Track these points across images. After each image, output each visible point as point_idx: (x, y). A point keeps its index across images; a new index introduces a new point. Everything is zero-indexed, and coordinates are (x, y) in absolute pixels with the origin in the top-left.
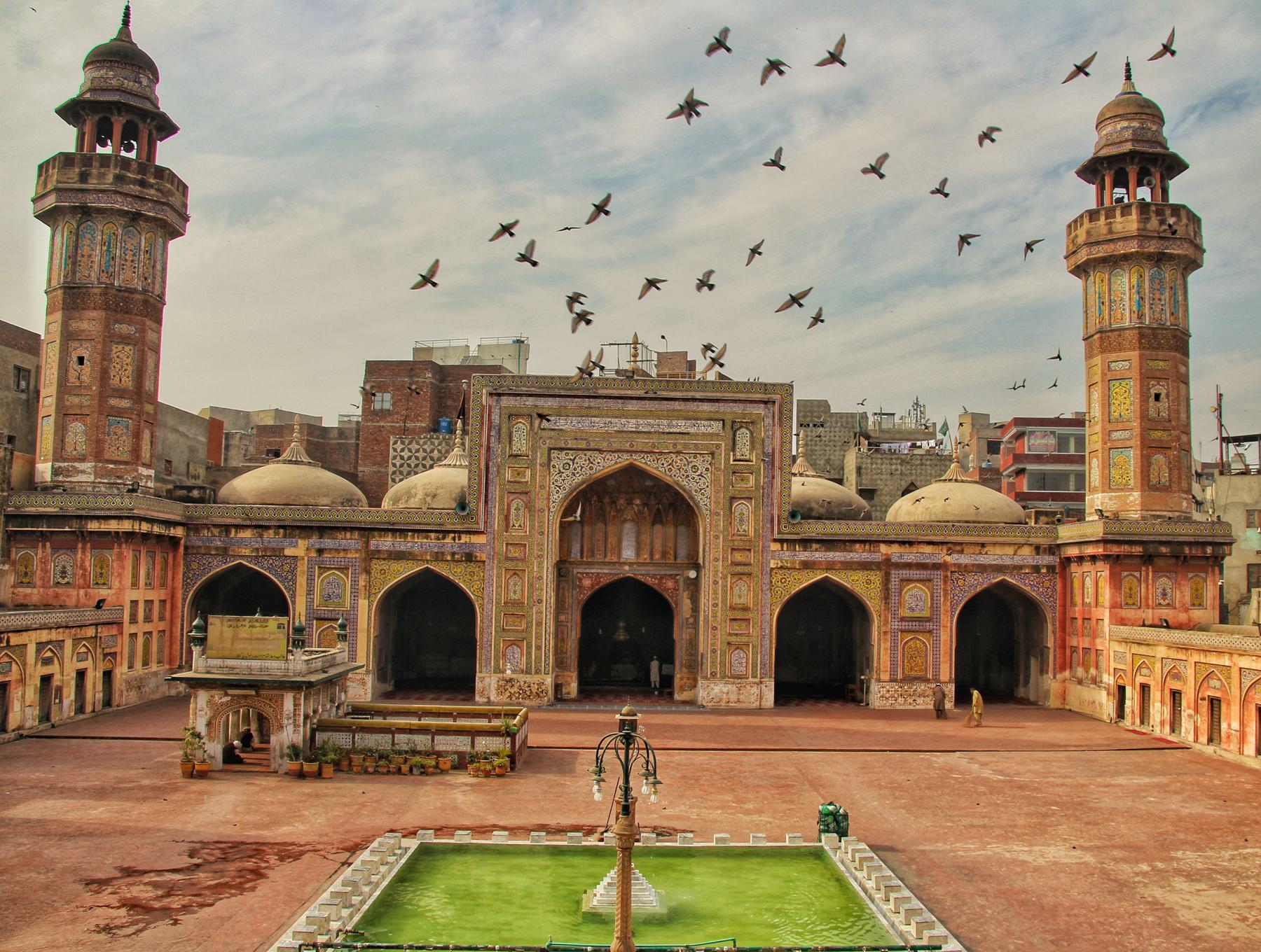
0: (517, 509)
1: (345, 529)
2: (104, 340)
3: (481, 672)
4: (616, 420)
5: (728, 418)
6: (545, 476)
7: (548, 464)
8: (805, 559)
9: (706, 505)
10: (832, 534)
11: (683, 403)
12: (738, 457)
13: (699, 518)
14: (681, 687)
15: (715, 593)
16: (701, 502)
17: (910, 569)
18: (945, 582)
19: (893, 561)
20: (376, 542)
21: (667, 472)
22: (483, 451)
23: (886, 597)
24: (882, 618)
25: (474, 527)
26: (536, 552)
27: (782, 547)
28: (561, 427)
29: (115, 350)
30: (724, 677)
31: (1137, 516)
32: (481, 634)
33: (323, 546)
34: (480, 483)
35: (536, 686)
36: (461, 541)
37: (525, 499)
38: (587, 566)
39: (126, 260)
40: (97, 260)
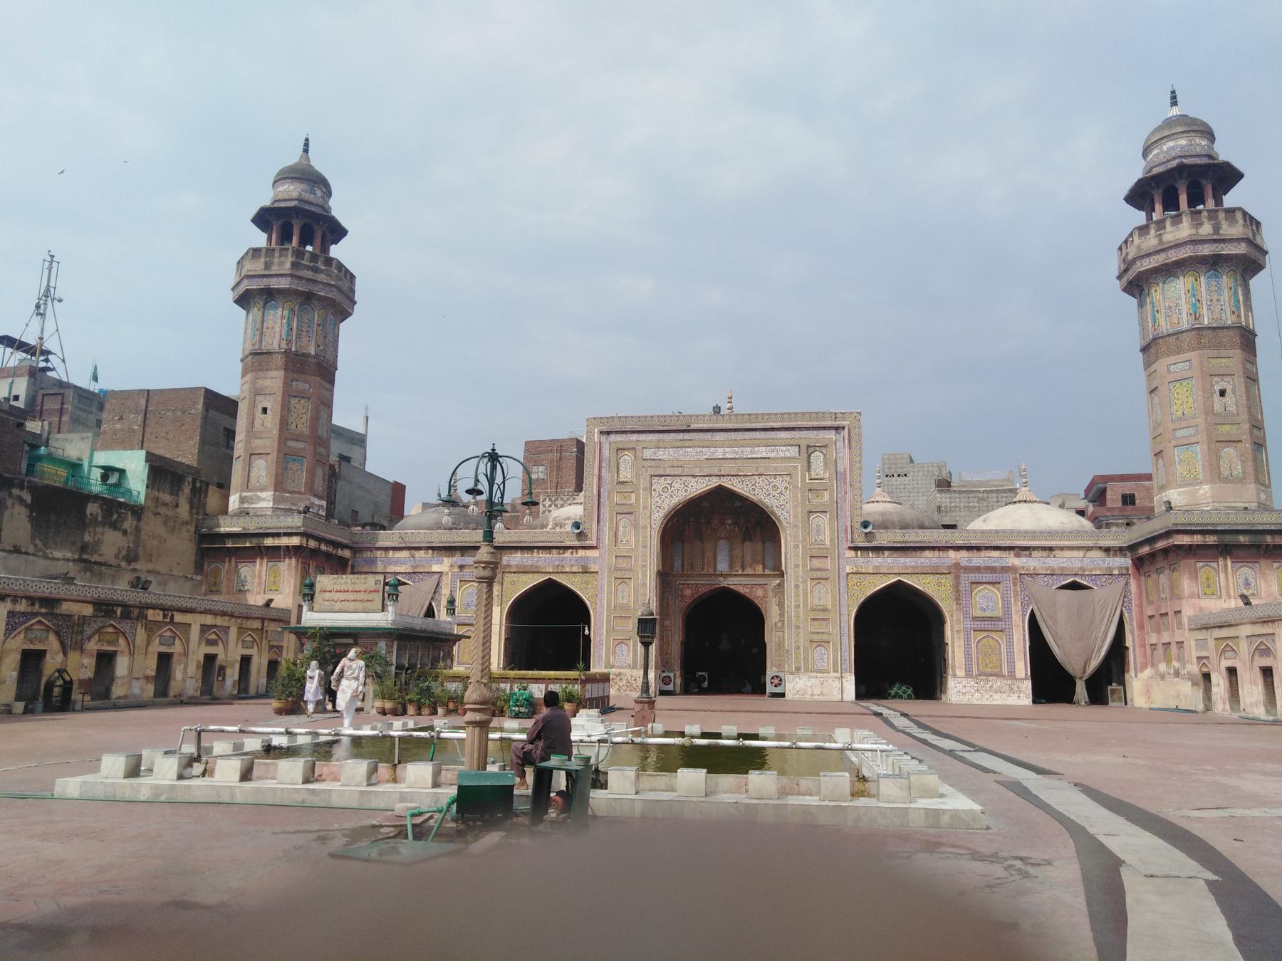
2: (283, 393)
6: (647, 499)
7: (650, 488)
9: (786, 519)
10: (903, 542)
16: (782, 517)
18: (1015, 584)
20: (507, 559)
21: (751, 492)
22: (596, 479)
25: (588, 543)
26: (640, 562)
29: (292, 402)
31: (1209, 508)
33: (464, 563)
36: (579, 555)
37: (631, 519)
39: (302, 331)
40: (278, 330)
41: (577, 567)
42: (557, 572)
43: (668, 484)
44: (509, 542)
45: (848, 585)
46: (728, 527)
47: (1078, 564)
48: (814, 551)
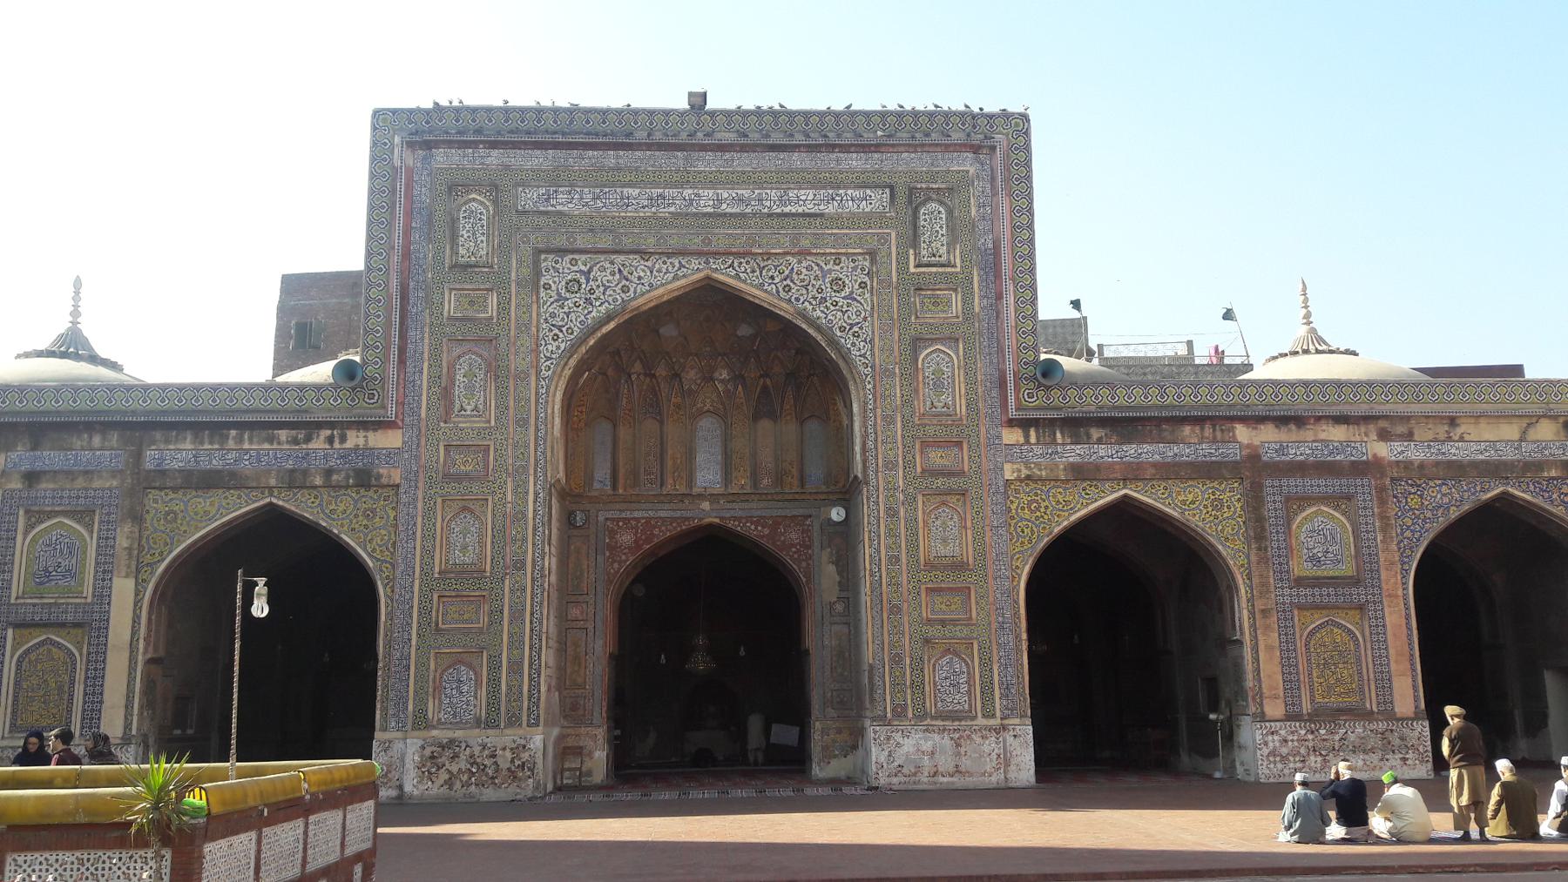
1: (89, 427)
3: (384, 729)
4: (673, 192)
7: (534, 282)
8: (1078, 459)
9: (863, 356)
10: (1129, 408)
13: (852, 387)
14: (825, 748)
15: (892, 533)
17: (1303, 477)
18: (1382, 502)
19: (1265, 458)
21: (782, 294)
23: (1258, 532)
24: (1256, 580)
25: (375, 414)
27: (1027, 437)
28: (559, 208)
30: (921, 716)
32: (388, 645)
33: (38, 466)
34: (388, 324)
35: (508, 754)
36: (349, 444)
38: (625, 506)
41: (343, 474)
43: (581, 272)
44: (164, 413)
47: (1510, 455)
48: (931, 430)
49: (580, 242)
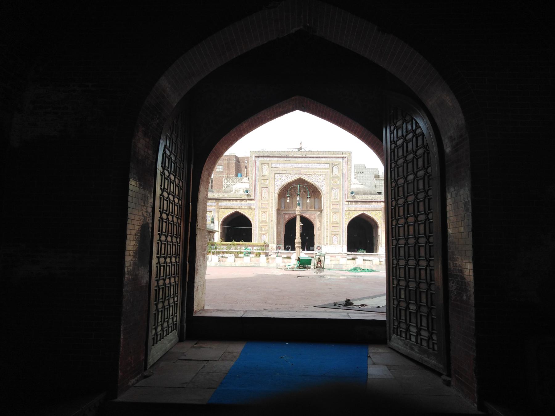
0: (265, 192)
5: (331, 163)
6: (273, 182)
11: (316, 159)
12: (334, 175)
15: (327, 218)
22: (254, 175)
25: (251, 198)
42: (239, 209)
45: (345, 214)
46: (302, 193)
49: (281, 173)
